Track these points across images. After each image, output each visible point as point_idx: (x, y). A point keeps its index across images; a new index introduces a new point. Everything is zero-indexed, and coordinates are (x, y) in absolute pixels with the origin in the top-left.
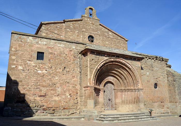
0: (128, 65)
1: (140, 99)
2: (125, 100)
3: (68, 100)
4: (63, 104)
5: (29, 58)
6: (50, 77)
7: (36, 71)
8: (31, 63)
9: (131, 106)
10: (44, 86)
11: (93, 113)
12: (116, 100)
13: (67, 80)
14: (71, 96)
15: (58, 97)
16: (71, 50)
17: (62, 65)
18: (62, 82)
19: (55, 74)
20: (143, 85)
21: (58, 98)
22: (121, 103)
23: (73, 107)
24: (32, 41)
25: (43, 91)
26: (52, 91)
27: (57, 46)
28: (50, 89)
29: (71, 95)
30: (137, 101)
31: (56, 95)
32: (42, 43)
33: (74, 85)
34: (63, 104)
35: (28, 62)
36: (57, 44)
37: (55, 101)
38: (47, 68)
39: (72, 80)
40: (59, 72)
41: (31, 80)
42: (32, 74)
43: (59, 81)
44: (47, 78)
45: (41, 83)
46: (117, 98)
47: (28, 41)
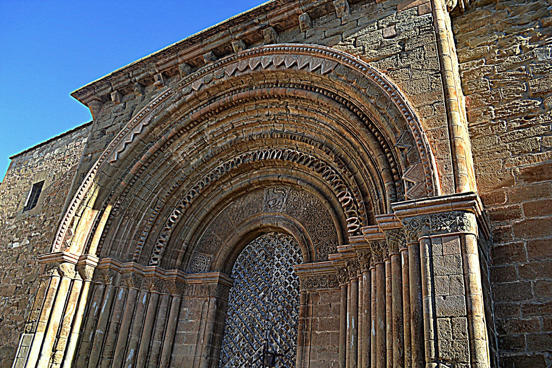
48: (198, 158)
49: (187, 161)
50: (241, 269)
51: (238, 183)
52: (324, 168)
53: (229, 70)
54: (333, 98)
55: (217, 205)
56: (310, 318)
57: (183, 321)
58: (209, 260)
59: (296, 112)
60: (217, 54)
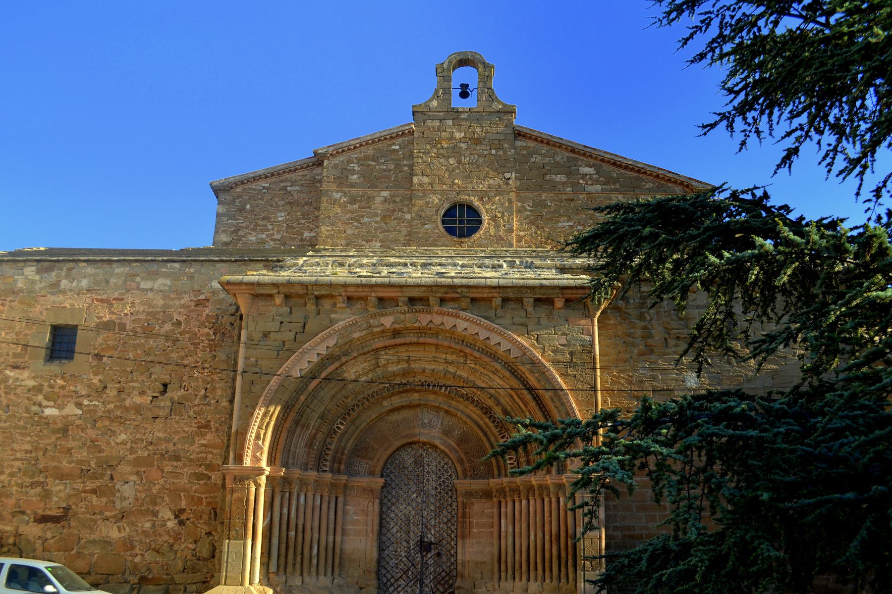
4: (138, 559)
5: (15, 355)
6: (92, 433)
7: (35, 408)
8: (21, 377)
10: (62, 475)
14: (181, 523)
15: (119, 528)
16: (202, 297)
17: (153, 377)
18: (146, 453)
19: (117, 417)
21: (120, 531)
24: (33, 282)
25: (55, 499)
26: (94, 499)
27: (138, 288)
28: (90, 486)
31: (115, 516)
32: (75, 284)
33: (202, 470)
34: (142, 558)
35: (8, 372)
36: (138, 279)
37: (106, 543)
38: (84, 393)
40: (138, 409)
41: (12, 450)
42: (21, 423)
43: (132, 451)
44: (78, 440)
45: (53, 458)
46: (464, 537)
47: (20, 285)
50: (391, 472)
51: (397, 401)
53: (424, 320)
54: (514, 372)
56: (467, 520)
57: (348, 518)
59: (473, 366)
60: (412, 300)
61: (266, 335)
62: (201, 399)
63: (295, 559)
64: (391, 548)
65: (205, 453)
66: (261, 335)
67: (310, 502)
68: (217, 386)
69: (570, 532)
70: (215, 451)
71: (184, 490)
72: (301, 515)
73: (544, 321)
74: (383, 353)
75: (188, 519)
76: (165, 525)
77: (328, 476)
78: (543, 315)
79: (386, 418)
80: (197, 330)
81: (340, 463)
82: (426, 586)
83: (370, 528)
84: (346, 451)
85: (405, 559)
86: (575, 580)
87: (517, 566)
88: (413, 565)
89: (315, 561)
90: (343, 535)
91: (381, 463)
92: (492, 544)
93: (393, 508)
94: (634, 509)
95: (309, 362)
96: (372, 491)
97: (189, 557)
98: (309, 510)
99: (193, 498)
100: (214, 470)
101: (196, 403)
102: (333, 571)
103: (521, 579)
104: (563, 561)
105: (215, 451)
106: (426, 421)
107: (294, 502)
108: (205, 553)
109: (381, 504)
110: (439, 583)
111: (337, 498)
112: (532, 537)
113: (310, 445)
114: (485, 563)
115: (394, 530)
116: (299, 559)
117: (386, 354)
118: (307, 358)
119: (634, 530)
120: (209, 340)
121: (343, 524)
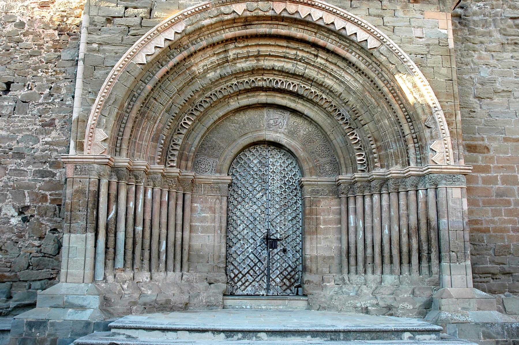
0: (351, 29)
1: (444, 233)
2: (361, 247)
3: (7, 236)
9: (389, 279)
11: (72, 306)
12: (308, 245)
13: (15, 142)
14: (25, 220)
20: (492, 153)
22: (336, 261)
23: (34, 273)
29: (28, 214)
30: (425, 247)
33: (46, 167)
39: (37, 141)
46: (312, 233)
48: (215, 71)
49: (206, 72)
51: (244, 101)
52: (336, 109)
55: (223, 116)
58: (215, 164)
61: (109, 20)
62: (45, 98)
63: (142, 255)
64: (238, 245)
65: (50, 150)
66: (104, 19)
67: (157, 198)
68: (62, 85)
69: (434, 223)
70: (59, 149)
71: (28, 187)
72: (148, 209)
73: (400, 13)
74: (232, 46)
75: (32, 216)
76: (9, 222)
77: (175, 171)
78: (398, 8)
79: (232, 118)
80: (41, 31)
81: (187, 160)
82: (273, 280)
83: (217, 225)
84: (193, 149)
85: (251, 256)
86: (440, 272)
87: (369, 260)
88: (260, 261)
89: (163, 257)
90: (190, 232)
91: (228, 162)
92: (340, 240)
93: (239, 207)
94: (481, 204)
95: (156, 47)
96: (219, 189)
97: (34, 254)
98: (156, 206)
99: (37, 195)
100: (59, 167)
101: (40, 101)
102: (181, 267)
103: (373, 273)
104: (425, 254)
105: (59, 149)
106: (272, 122)
107: (141, 196)
108: (50, 249)
109: (228, 202)
110: (285, 277)
111: (184, 194)
112: (386, 231)
113: (156, 139)
114: (333, 257)
115: (241, 227)
116: (147, 254)
117: (236, 47)
118: (154, 43)
119: (482, 224)
120: (54, 41)
121: (191, 221)
